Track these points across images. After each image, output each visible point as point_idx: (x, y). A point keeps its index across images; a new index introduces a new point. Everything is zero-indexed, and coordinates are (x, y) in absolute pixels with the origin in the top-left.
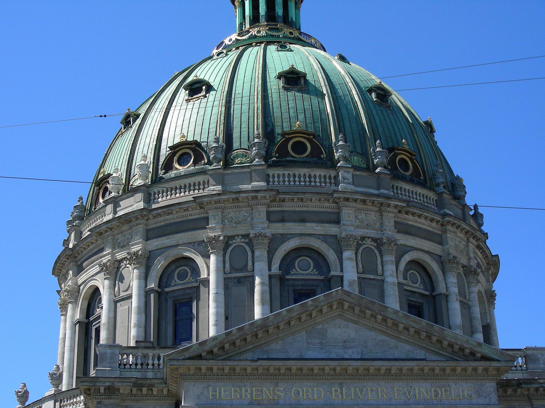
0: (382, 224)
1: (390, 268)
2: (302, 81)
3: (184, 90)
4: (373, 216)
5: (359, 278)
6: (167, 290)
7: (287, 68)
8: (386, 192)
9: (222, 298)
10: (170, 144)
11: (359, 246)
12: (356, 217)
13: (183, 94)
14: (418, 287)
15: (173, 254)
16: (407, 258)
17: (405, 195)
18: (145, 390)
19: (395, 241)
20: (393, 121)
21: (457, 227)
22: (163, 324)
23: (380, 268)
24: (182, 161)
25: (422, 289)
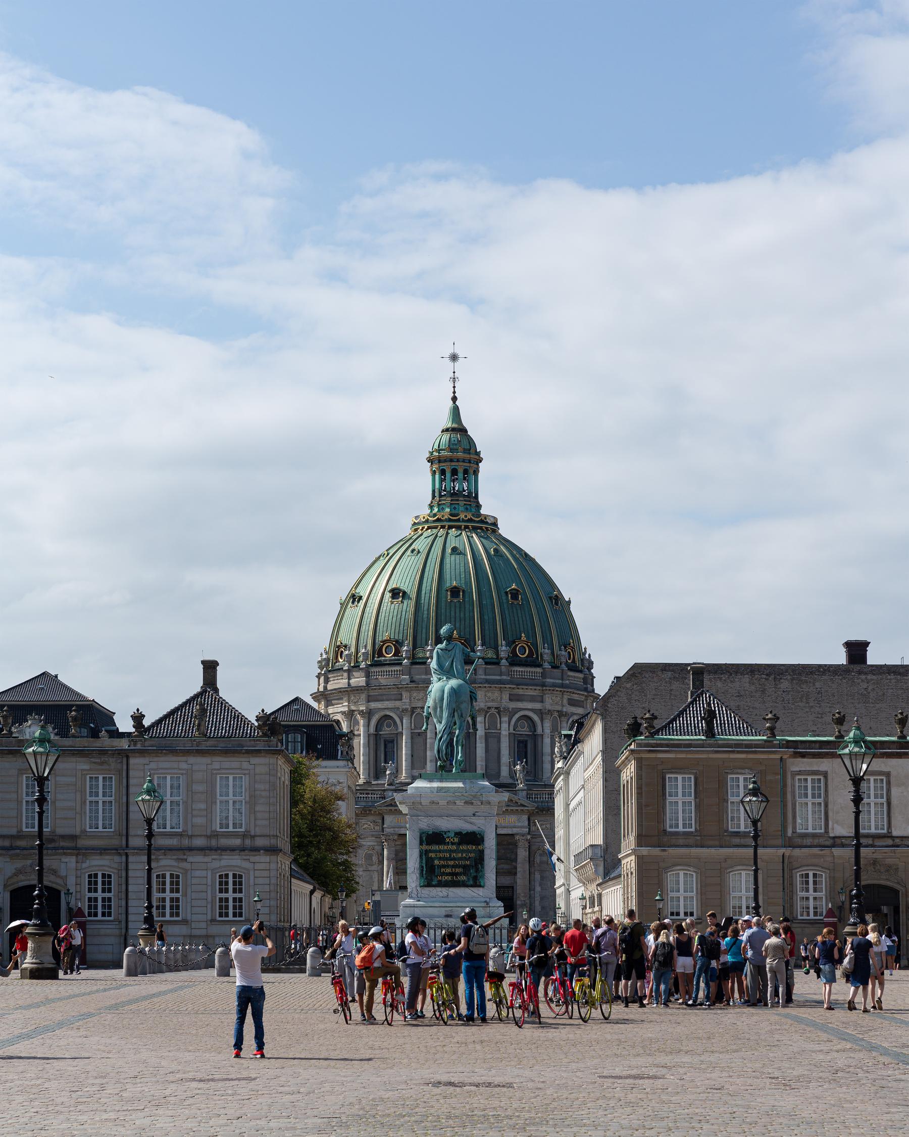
0: (501, 698)
1: (505, 726)
2: (461, 593)
3: (388, 593)
4: (497, 694)
5: (485, 733)
6: (380, 733)
7: (454, 584)
8: (504, 677)
9: (409, 745)
10: (380, 640)
11: (487, 712)
12: (485, 695)
13: (388, 595)
14: (525, 730)
15: (382, 713)
16: (517, 716)
17: (519, 675)
18: (368, 812)
19: (509, 708)
20: (520, 615)
21: (553, 690)
22: (378, 753)
23: (499, 725)
24: (387, 650)
25: (528, 731)
